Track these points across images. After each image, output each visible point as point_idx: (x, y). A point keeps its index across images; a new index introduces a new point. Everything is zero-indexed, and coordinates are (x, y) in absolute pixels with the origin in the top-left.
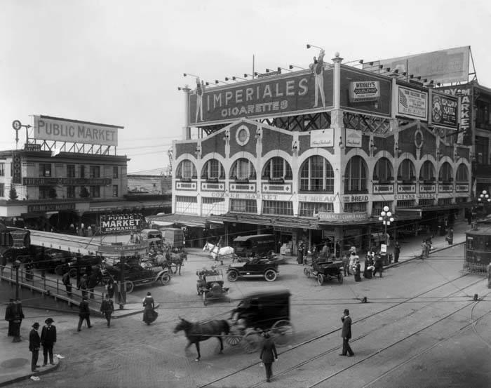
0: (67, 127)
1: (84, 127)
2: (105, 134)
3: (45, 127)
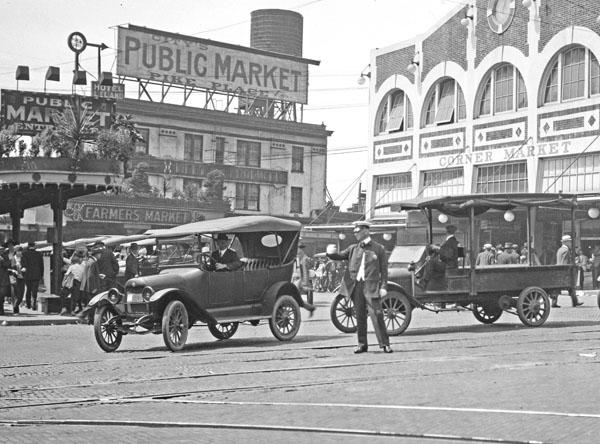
0: (190, 53)
1: (228, 58)
2: (277, 73)
3: (141, 50)
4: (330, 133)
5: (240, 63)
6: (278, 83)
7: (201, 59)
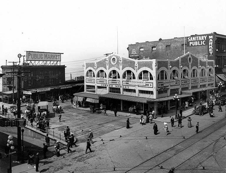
0: (40, 55)
1: (47, 54)
4: (66, 67)
5: (49, 55)
6: (56, 58)
7: (42, 56)
